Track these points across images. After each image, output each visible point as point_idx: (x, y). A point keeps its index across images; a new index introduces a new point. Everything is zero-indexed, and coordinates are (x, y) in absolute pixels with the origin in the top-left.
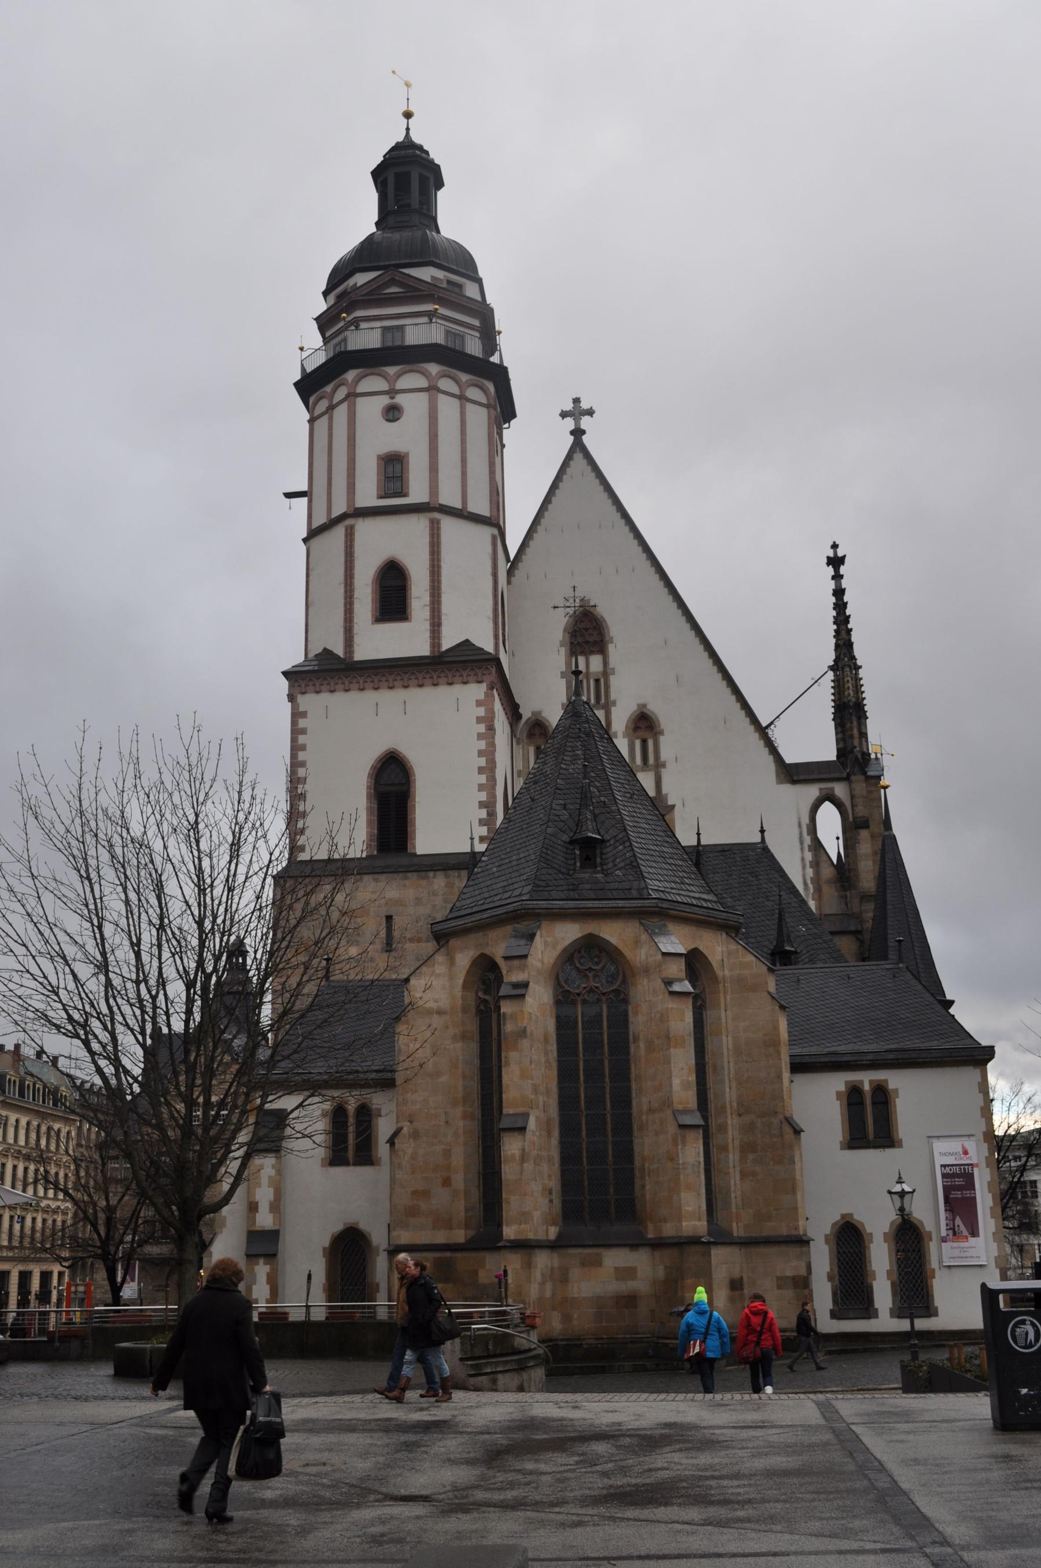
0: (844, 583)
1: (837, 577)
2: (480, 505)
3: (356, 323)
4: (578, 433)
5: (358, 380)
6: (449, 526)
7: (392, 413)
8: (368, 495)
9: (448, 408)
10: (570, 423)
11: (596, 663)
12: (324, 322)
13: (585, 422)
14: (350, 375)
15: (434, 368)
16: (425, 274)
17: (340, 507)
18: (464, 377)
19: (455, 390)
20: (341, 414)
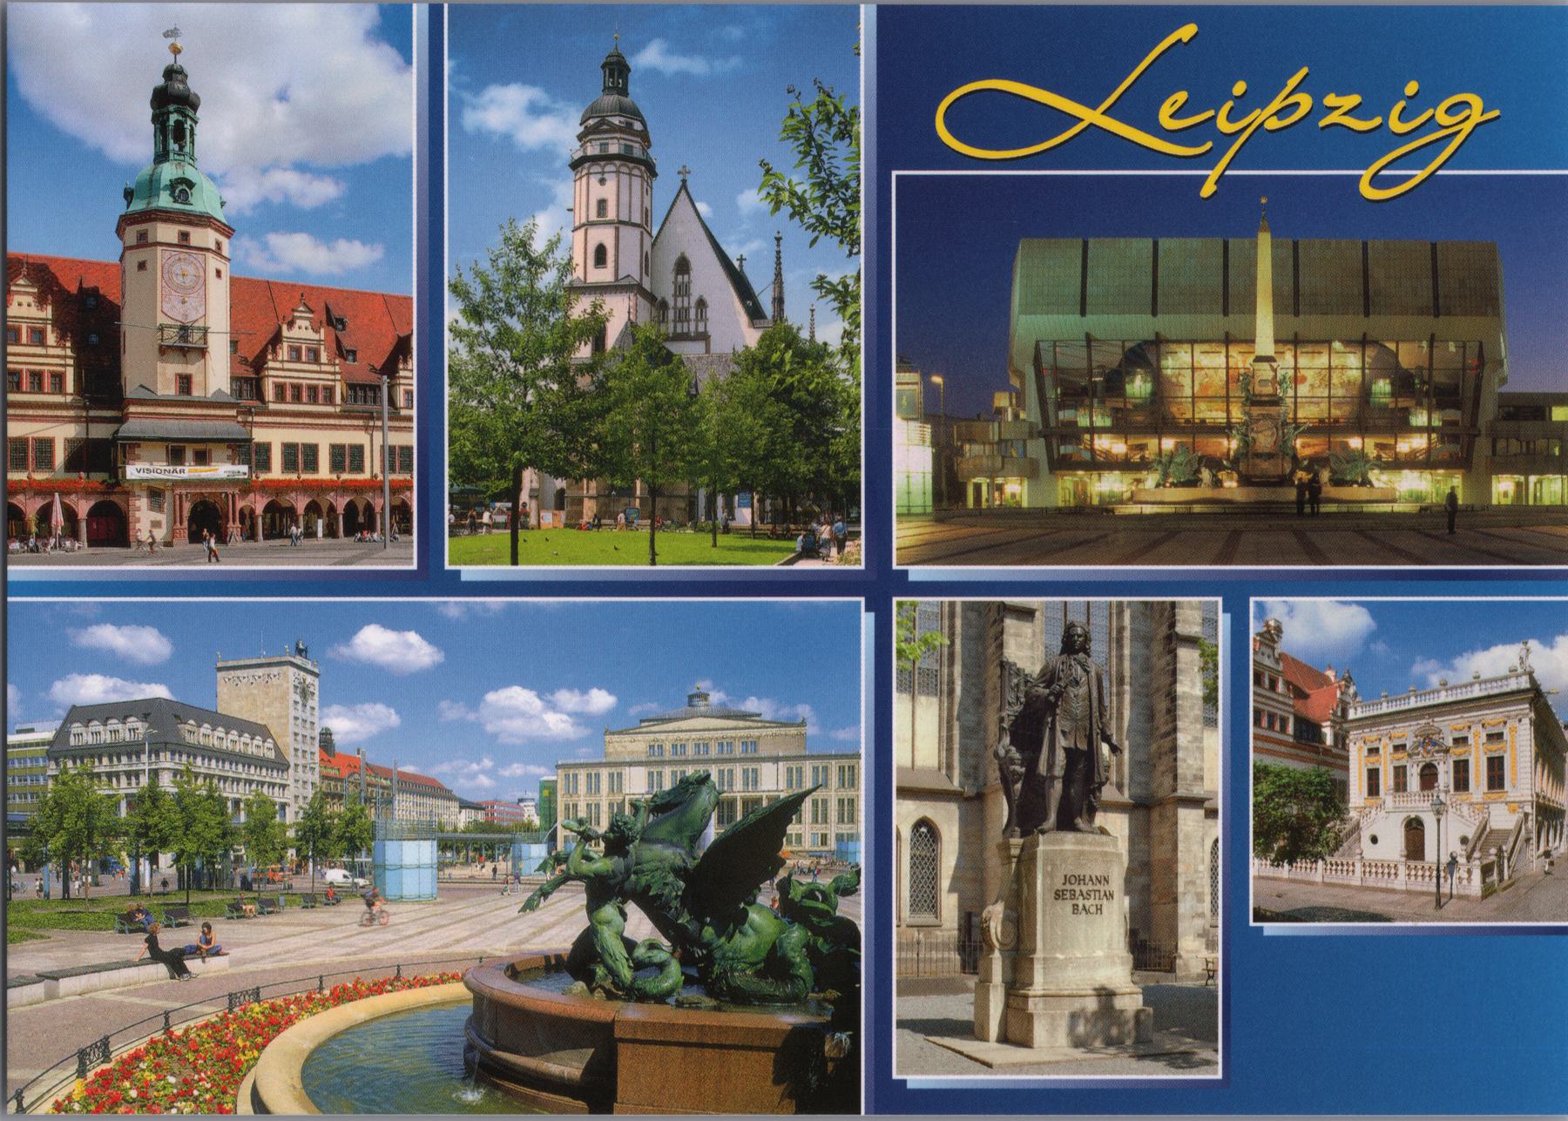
0: (782, 248)
1: (778, 245)
2: (637, 219)
3: (590, 141)
4: (684, 181)
5: (589, 168)
6: (623, 229)
7: (602, 181)
8: (593, 217)
9: (625, 179)
10: (681, 177)
11: (686, 277)
12: (580, 137)
13: (688, 177)
14: (587, 165)
15: (618, 163)
16: (616, 121)
17: (584, 220)
18: (631, 165)
19: (627, 171)
20: (584, 179)
